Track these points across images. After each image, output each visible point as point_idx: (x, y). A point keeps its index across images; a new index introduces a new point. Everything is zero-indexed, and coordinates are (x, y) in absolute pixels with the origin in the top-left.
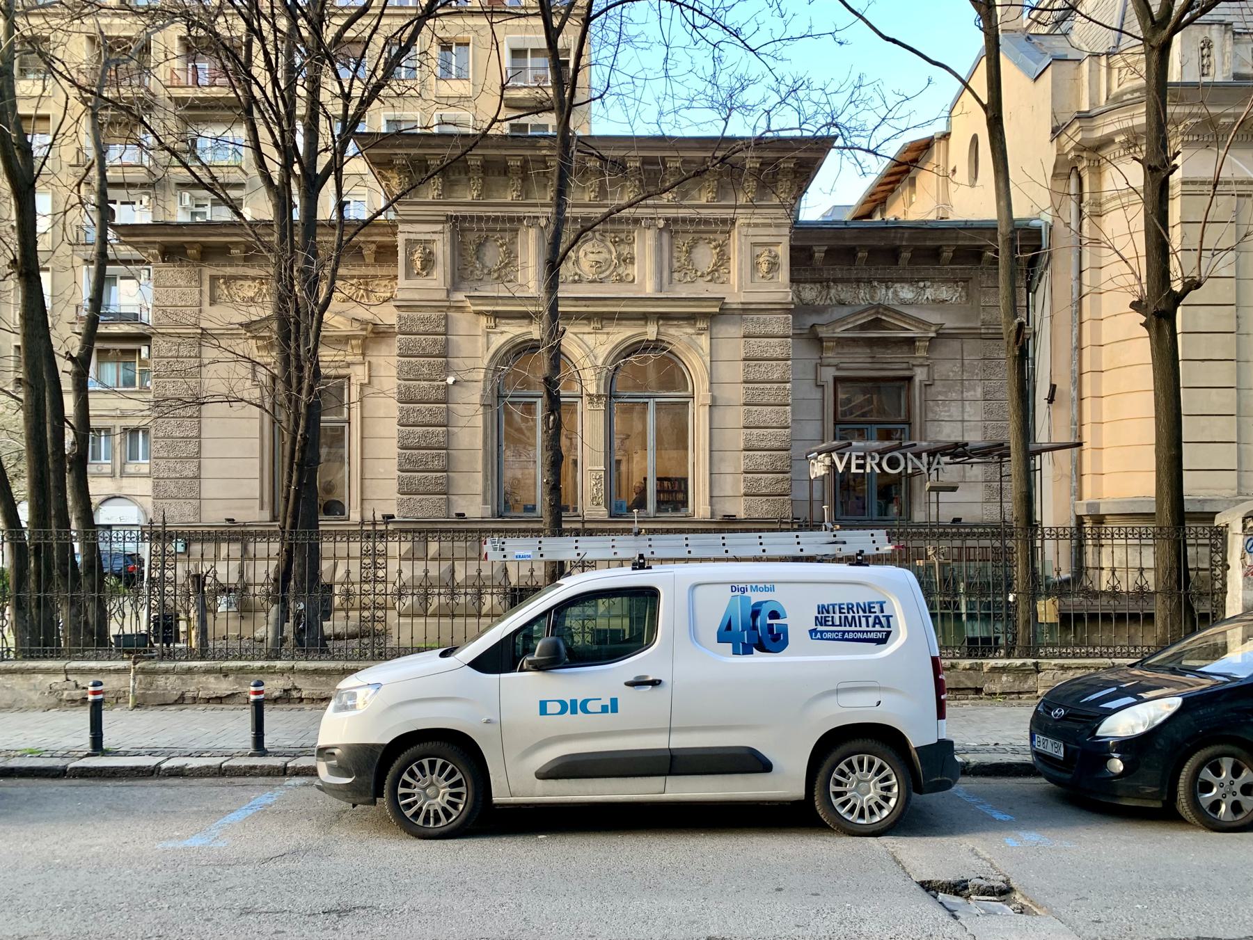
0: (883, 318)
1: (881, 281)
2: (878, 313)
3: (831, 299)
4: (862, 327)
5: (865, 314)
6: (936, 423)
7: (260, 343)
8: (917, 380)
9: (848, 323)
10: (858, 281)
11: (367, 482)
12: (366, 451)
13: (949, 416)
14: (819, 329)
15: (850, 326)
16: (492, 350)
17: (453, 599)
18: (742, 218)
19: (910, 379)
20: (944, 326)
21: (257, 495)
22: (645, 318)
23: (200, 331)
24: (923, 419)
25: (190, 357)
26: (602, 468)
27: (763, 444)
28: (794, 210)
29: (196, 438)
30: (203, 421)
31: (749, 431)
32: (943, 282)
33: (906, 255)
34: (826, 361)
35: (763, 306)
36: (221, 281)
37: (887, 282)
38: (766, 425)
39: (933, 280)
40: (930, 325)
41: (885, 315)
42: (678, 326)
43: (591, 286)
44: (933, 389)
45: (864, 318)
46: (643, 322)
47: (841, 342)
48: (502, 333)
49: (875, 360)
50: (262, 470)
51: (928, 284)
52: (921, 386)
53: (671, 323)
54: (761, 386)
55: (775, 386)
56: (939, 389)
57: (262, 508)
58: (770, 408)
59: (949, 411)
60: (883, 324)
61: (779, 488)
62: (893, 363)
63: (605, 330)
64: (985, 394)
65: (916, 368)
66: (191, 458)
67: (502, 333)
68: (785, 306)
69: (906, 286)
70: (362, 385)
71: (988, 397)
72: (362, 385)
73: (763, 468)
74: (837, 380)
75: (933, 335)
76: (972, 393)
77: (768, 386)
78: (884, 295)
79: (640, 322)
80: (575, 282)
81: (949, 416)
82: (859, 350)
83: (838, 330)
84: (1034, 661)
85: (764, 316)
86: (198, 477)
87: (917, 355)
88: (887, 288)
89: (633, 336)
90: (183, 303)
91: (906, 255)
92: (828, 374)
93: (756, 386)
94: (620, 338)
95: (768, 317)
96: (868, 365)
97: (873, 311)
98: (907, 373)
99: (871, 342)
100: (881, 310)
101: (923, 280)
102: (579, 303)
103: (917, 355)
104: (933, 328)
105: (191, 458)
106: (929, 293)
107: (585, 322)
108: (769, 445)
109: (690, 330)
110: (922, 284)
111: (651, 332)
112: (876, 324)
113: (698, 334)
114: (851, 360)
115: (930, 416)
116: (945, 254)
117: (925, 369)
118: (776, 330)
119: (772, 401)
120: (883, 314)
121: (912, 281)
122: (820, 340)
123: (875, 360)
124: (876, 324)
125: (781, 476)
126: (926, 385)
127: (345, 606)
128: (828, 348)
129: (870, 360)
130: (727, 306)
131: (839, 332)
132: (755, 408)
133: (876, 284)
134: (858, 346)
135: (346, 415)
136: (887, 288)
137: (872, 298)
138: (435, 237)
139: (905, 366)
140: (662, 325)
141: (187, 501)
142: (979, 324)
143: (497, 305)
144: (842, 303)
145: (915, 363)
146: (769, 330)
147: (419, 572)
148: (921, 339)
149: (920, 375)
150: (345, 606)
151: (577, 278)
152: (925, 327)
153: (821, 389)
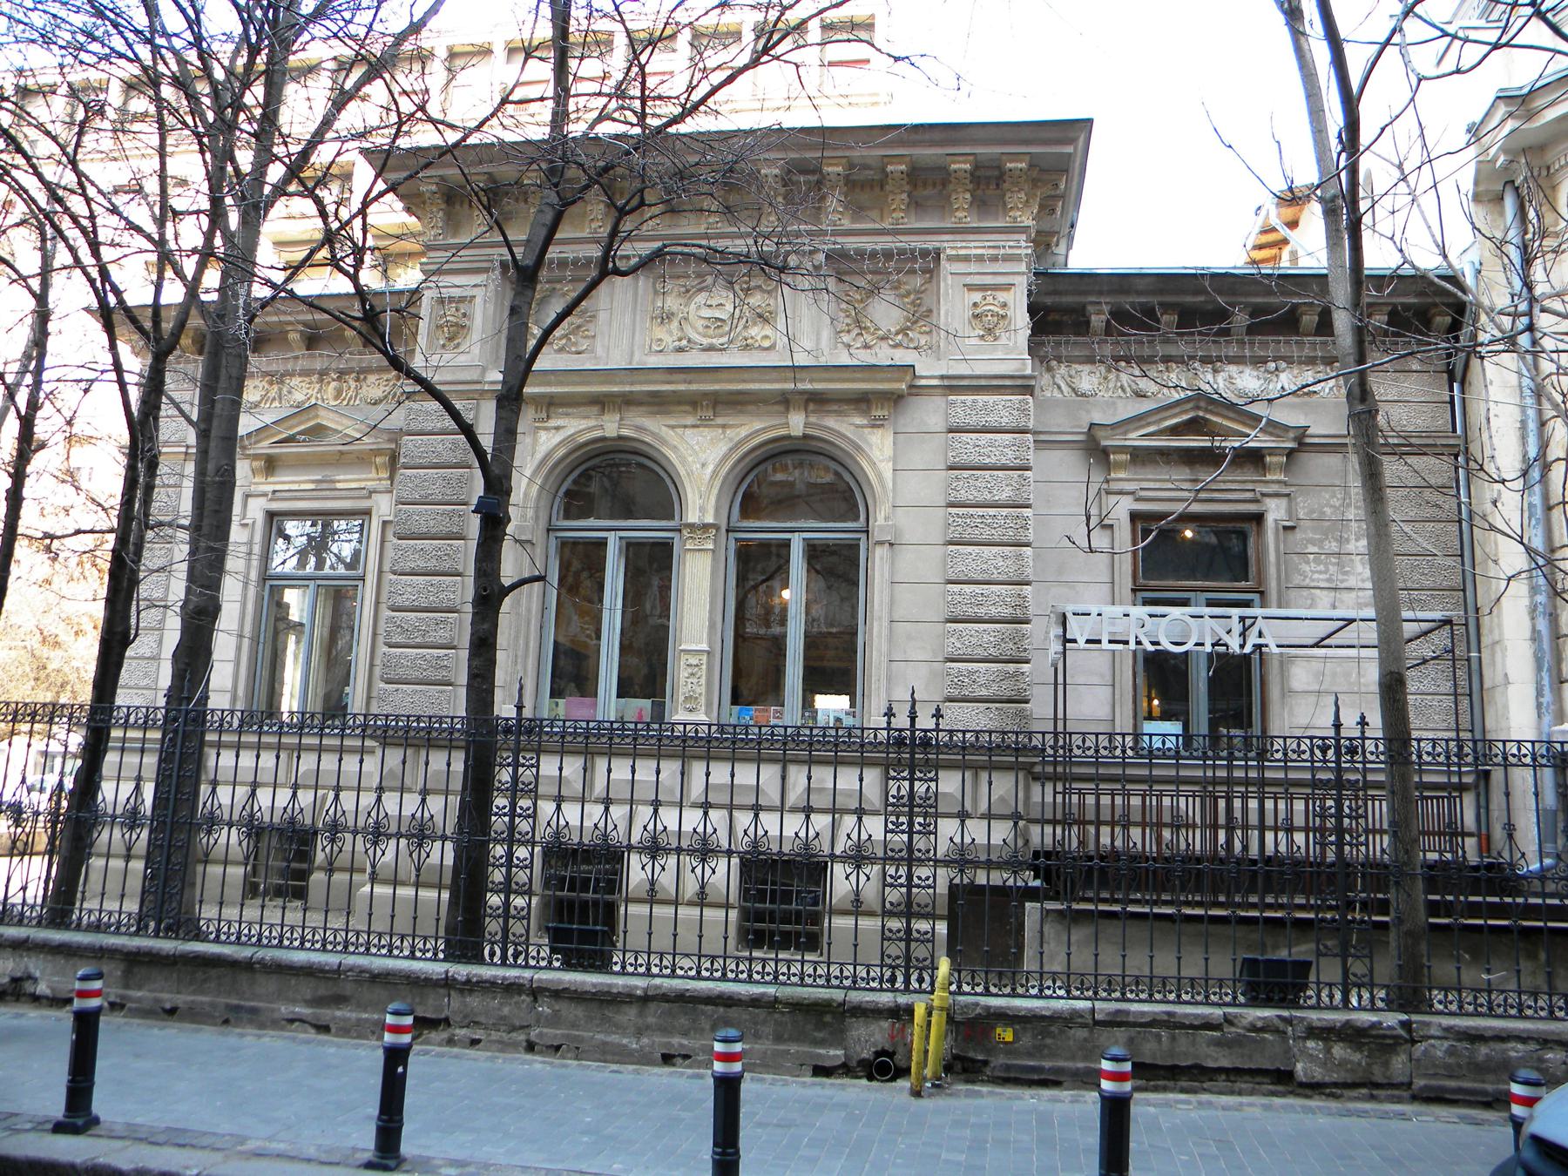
1: (1205, 360)
2: (1198, 408)
3: (1122, 387)
4: (1175, 431)
5: (1177, 410)
6: (1305, 593)
7: (256, 464)
8: (1270, 519)
9: (1149, 424)
10: (1167, 359)
13: (1328, 580)
14: (1100, 433)
15: (1152, 429)
16: (539, 456)
18: (950, 246)
19: (1258, 518)
20: (1309, 432)
22: (785, 401)
24: (1284, 585)
27: (982, 612)
28: (1047, 240)
31: (956, 588)
32: (1307, 363)
33: (1241, 319)
34: (1114, 486)
35: (983, 382)
38: (986, 577)
39: (1289, 361)
40: (1286, 428)
42: (839, 413)
44: (1298, 535)
45: (1174, 416)
46: (781, 408)
47: (1141, 457)
48: (557, 428)
51: (1283, 365)
52: (1277, 529)
53: (827, 408)
54: (980, 511)
55: (1005, 511)
59: (1326, 572)
61: (1006, 689)
63: (719, 421)
67: (557, 428)
68: (1019, 382)
70: (385, 523)
72: (385, 523)
73: (982, 653)
74: (1135, 517)
77: (992, 511)
79: (777, 408)
81: (1328, 580)
83: (1133, 435)
84: (1404, 1017)
85: (985, 398)
87: (1269, 477)
88: (1215, 371)
89: (764, 430)
92: (1121, 509)
93: (971, 511)
94: (744, 432)
95: (991, 399)
98: (1252, 508)
100: (1202, 404)
102: (676, 377)
103: (1269, 477)
104: (1291, 435)
107: (688, 408)
108: (994, 611)
109: (859, 420)
110: (1272, 365)
111: (797, 423)
112: (1194, 426)
113: (873, 426)
114: (1157, 485)
116: (1305, 318)
117: (1283, 502)
118: (1005, 420)
119: (997, 538)
120: (1206, 411)
121: (1258, 362)
122: (1105, 452)
124: (1194, 426)
125: (1011, 667)
126: (1286, 528)
128: (1120, 466)
130: (923, 382)
131: (1135, 439)
132: (970, 549)
135: (360, 571)
136: (1215, 371)
138: (475, 292)
139: (1249, 495)
140: (813, 412)
143: (549, 384)
144: (1140, 395)
145: (1265, 490)
146: (992, 420)
148: (1273, 451)
149: (1275, 512)
151: (684, 342)
153: (1108, 532)
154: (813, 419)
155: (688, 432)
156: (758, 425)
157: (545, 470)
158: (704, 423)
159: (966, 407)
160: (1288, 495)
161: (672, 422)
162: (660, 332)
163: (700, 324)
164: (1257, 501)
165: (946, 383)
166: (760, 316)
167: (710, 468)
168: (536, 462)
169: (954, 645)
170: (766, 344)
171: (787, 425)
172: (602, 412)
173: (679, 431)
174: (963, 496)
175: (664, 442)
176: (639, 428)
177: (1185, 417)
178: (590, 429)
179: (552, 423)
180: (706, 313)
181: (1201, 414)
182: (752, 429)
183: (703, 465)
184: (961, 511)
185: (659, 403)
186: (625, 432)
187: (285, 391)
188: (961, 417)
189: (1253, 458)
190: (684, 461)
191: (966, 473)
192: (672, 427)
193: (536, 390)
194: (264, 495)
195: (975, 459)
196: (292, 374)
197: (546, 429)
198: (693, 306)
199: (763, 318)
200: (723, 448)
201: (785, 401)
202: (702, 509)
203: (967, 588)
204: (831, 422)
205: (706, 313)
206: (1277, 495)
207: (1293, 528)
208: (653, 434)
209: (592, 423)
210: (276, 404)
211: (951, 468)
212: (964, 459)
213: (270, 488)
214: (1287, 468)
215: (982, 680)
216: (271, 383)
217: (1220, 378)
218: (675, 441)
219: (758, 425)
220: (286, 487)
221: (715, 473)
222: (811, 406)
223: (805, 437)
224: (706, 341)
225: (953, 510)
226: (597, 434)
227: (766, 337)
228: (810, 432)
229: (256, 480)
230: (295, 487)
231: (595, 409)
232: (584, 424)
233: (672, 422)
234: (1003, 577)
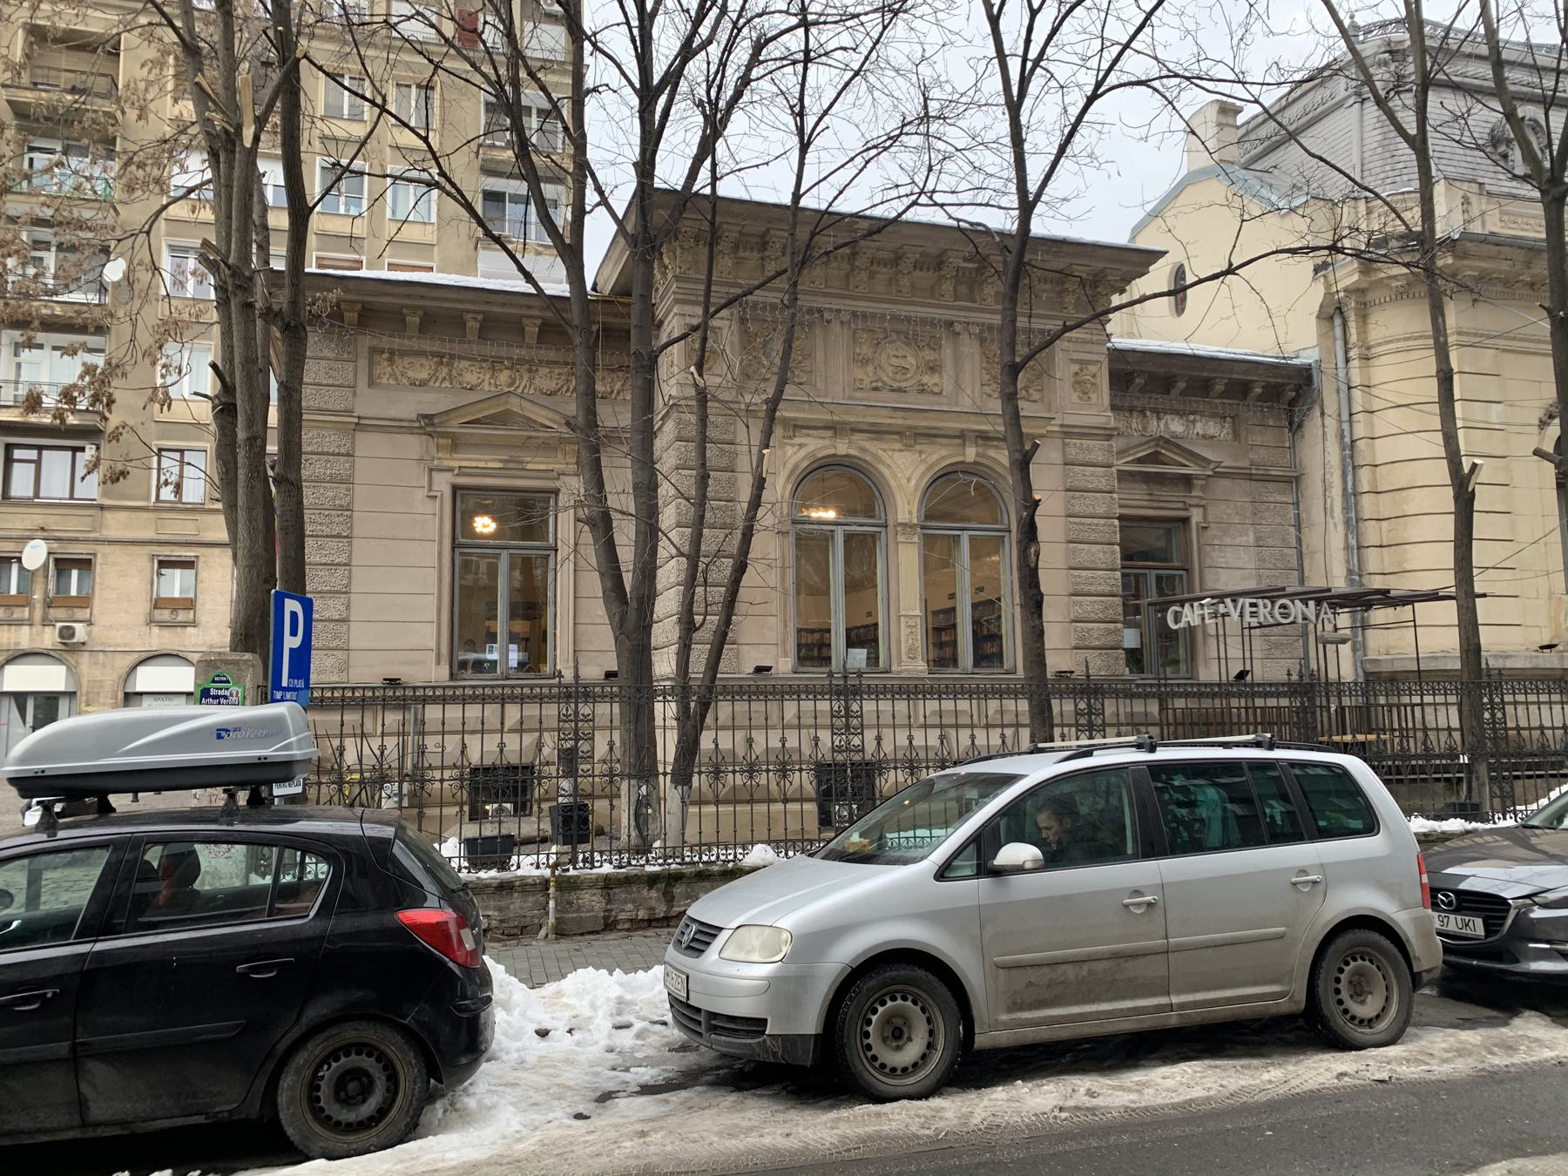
2: (1158, 445)
4: (1140, 461)
6: (1214, 570)
8: (1194, 520)
10: (1131, 410)
11: (581, 628)
12: (580, 588)
16: (790, 465)
17: (751, 778)
19: (1185, 521)
21: (433, 645)
23: (356, 420)
25: (338, 454)
26: (917, 612)
27: (1092, 589)
29: (345, 565)
30: (355, 542)
31: (1076, 573)
35: (1087, 431)
36: (385, 356)
37: (1158, 413)
38: (1094, 566)
39: (1202, 414)
40: (1209, 462)
42: (997, 447)
43: (895, 395)
44: (1209, 533)
46: (959, 441)
48: (801, 446)
50: (439, 611)
51: (1198, 417)
54: (1088, 521)
55: (1102, 521)
56: (1214, 532)
57: (438, 662)
60: (1161, 458)
61: (1110, 641)
62: (1169, 503)
63: (918, 447)
64: (1258, 539)
65: (1192, 509)
66: (337, 592)
67: (801, 446)
69: (1176, 418)
71: (1261, 543)
75: (1210, 473)
76: (1244, 538)
77: (1095, 521)
78: (1156, 427)
80: (876, 389)
82: (1136, 485)
86: (345, 620)
89: (944, 458)
90: (330, 382)
91: (1181, 385)
93: (1083, 520)
94: (935, 457)
96: (1145, 503)
97: (1152, 444)
98: (1183, 514)
99: (1147, 478)
104: (1212, 466)
105: (337, 592)
106: (1199, 428)
111: (971, 454)
112: (1154, 458)
115: (1208, 562)
116: (1218, 387)
119: (1099, 539)
124: (1154, 458)
127: (608, 790)
129: (1147, 497)
133: (1148, 413)
134: (1135, 481)
137: (1145, 429)
139: (1181, 505)
141: (330, 653)
142: (1247, 464)
143: (803, 411)
146: (1092, 457)
147: (775, 743)
148: (1197, 477)
149: (1196, 516)
150: (608, 790)
151: (880, 384)
154: (980, 450)
155: (896, 454)
156: (944, 452)
157: (793, 478)
158: (908, 447)
159: (1076, 447)
161: (885, 446)
162: (859, 374)
163: (890, 370)
164: (1186, 509)
165: (1065, 429)
166: (931, 368)
167: (913, 482)
168: (787, 471)
169: (1077, 611)
170: (936, 390)
171: (964, 454)
172: (835, 435)
173: (890, 453)
174: (1078, 509)
175: (880, 460)
176: (863, 450)
178: (826, 448)
179: (797, 440)
180: (896, 362)
182: (940, 455)
183: (909, 480)
184: (1077, 520)
185: (877, 432)
186: (852, 452)
187: (454, 373)
188: (1072, 453)
189: (1187, 481)
190: (896, 477)
191: (1078, 494)
192: (884, 450)
193: (787, 414)
194: (450, 470)
195: (1083, 485)
196: (460, 358)
197: (793, 445)
198: (884, 356)
199: (933, 368)
200: (922, 468)
201: (962, 436)
202: (910, 513)
203: (1084, 573)
204: (991, 453)
205: (896, 362)
206: (1197, 506)
207: (1205, 528)
208: (873, 454)
209: (827, 442)
210: (447, 384)
211: (1068, 490)
212: (1077, 484)
213: (456, 464)
214: (1203, 488)
215: (1096, 635)
216: (441, 363)
217: (1162, 423)
218: (889, 461)
219: (944, 452)
220: (474, 464)
221: (917, 486)
222: (980, 442)
223: (975, 463)
224: (895, 385)
225: (1072, 519)
226: (831, 451)
227: (936, 384)
228: (978, 459)
229: (440, 455)
230: (482, 465)
231: (829, 433)
232: (821, 443)
233: (885, 446)
234: (1104, 566)
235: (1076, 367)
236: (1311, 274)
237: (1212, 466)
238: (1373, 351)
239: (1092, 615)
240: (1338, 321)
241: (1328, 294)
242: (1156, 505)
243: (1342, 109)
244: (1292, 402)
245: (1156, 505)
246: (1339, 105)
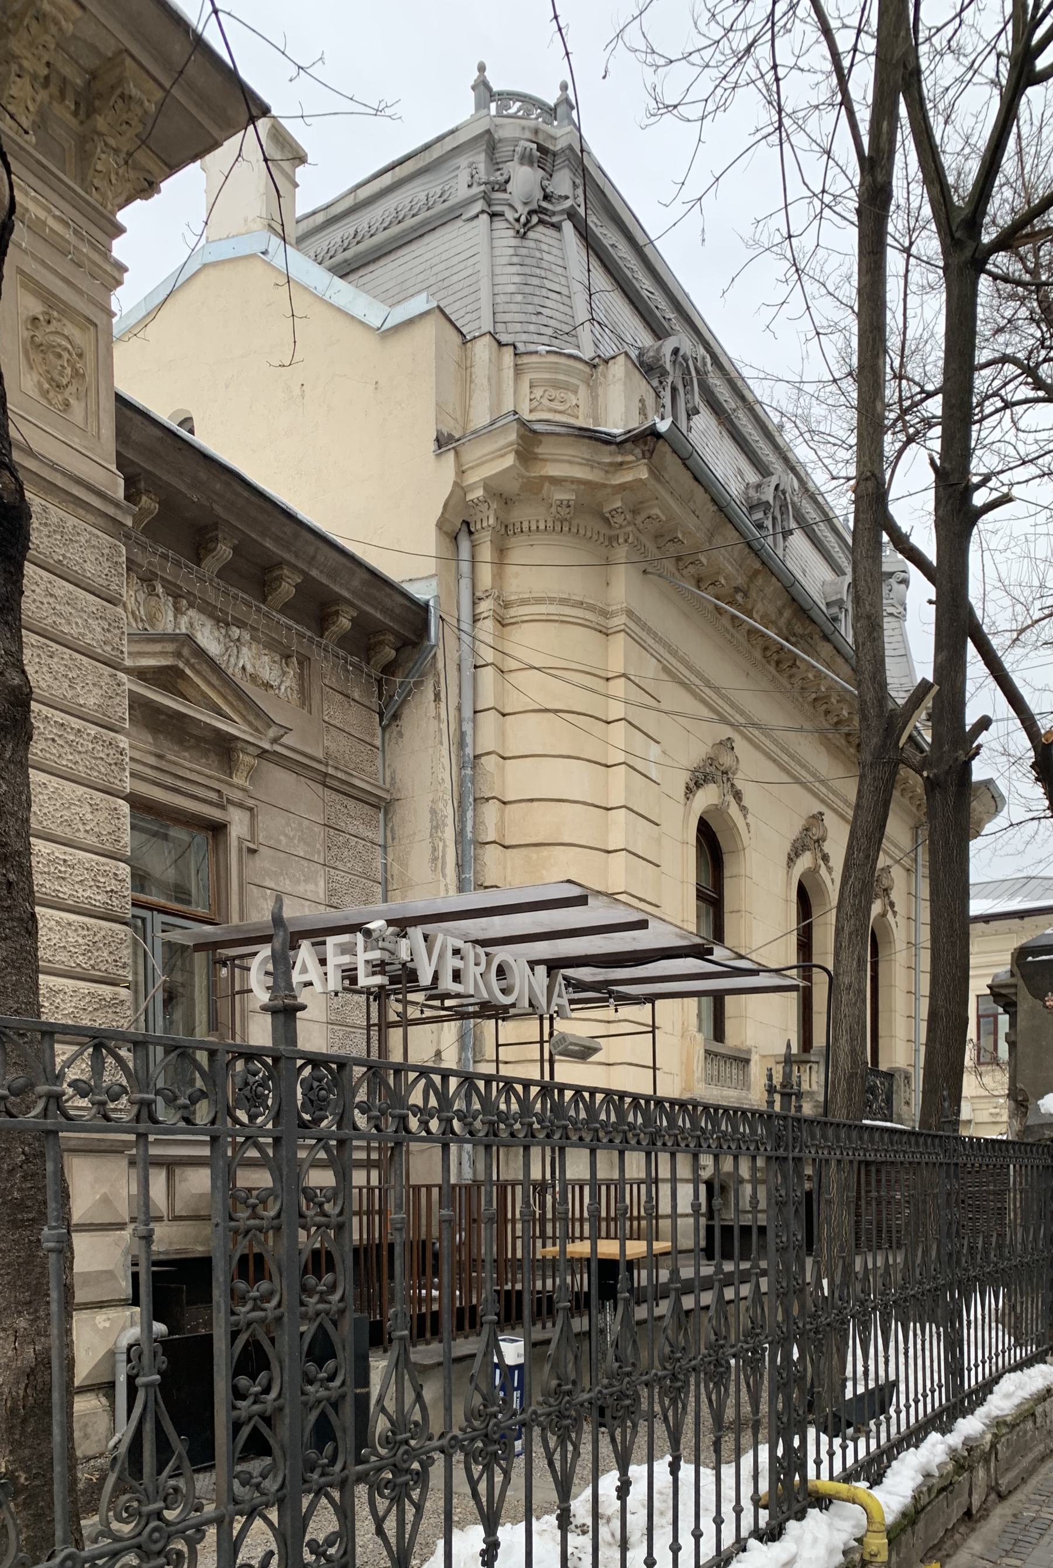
0: (188, 671)
19: (218, 830)
35: (59, 481)
40: (270, 722)
41: (192, 667)
45: (153, 654)
49: (163, 765)
52: (240, 850)
55: (93, 730)
56: (266, 864)
58: (81, 790)
60: (182, 685)
64: (331, 893)
65: (231, 809)
76: (311, 887)
77: (76, 723)
91: (224, 551)
97: (170, 647)
98: (215, 814)
100: (186, 652)
101: (241, 624)
104: (272, 732)
110: (235, 632)
119: (81, 771)
120: (187, 663)
123: (163, 765)
129: (152, 760)
133: (160, 590)
139: (213, 796)
149: (238, 826)
152: (259, 724)
160: (251, 809)
164: (223, 807)
177: (164, 662)
181: (181, 665)
206: (240, 806)
207: (252, 851)
214: (252, 773)
234: (91, 840)
235: (37, 308)
236: (432, 446)
237: (272, 732)
238: (512, 612)
239: (62, 956)
240: (465, 545)
241: (459, 488)
242: (169, 781)
243: (459, 223)
244: (389, 669)
245: (169, 781)
246: (452, 215)
